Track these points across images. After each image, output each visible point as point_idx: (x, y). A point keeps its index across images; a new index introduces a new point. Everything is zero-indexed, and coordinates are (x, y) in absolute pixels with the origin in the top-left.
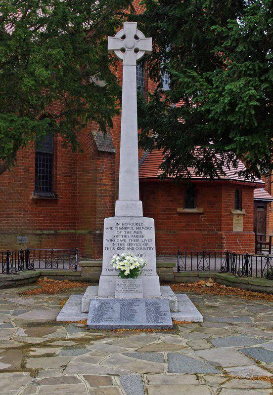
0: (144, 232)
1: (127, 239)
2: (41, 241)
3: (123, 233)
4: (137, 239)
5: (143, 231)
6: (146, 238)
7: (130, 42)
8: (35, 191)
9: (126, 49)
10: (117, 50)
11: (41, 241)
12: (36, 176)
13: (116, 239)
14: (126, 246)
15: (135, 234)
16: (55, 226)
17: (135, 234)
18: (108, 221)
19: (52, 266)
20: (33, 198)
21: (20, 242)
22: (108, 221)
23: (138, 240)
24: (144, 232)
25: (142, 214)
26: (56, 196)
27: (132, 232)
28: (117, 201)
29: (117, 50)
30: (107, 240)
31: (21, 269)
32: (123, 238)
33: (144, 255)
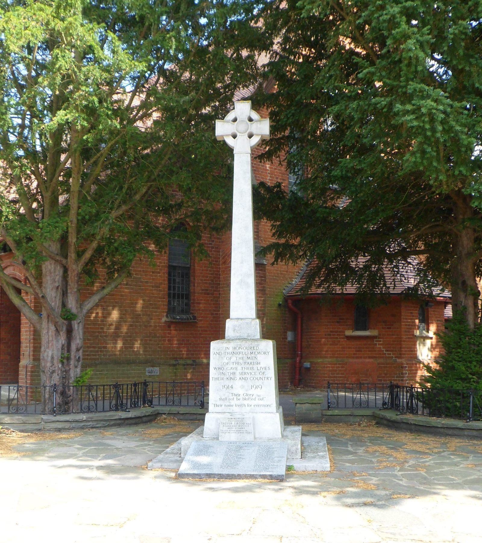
0: (260, 358)
1: (239, 368)
2: (175, 373)
3: (234, 359)
4: (251, 366)
5: (259, 356)
6: (262, 365)
7: (241, 127)
8: (168, 313)
9: (238, 134)
10: (227, 135)
11: (175, 373)
12: (169, 295)
13: (225, 368)
14: (238, 376)
15: (249, 361)
16: (193, 354)
17: (249, 361)
18: (215, 346)
19: (173, 403)
20: (166, 322)
21: (150, 374)
22: (215, 346)
23: (252, 368)
24: (260, 358)
25: (258, 336)
26: (195, 318)
27: (245, 358)
28: (228, 321)
29: (227, 135)
30: (215, 368)
31: (135, 406)
32: (234, 366)
33: (260, 387)
